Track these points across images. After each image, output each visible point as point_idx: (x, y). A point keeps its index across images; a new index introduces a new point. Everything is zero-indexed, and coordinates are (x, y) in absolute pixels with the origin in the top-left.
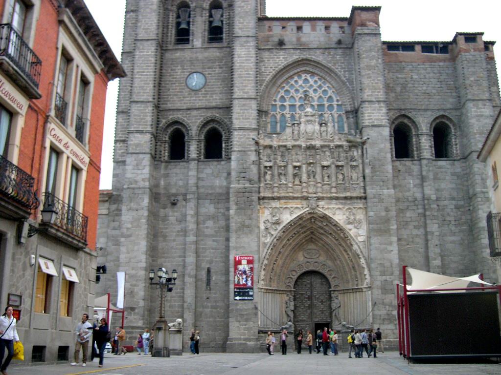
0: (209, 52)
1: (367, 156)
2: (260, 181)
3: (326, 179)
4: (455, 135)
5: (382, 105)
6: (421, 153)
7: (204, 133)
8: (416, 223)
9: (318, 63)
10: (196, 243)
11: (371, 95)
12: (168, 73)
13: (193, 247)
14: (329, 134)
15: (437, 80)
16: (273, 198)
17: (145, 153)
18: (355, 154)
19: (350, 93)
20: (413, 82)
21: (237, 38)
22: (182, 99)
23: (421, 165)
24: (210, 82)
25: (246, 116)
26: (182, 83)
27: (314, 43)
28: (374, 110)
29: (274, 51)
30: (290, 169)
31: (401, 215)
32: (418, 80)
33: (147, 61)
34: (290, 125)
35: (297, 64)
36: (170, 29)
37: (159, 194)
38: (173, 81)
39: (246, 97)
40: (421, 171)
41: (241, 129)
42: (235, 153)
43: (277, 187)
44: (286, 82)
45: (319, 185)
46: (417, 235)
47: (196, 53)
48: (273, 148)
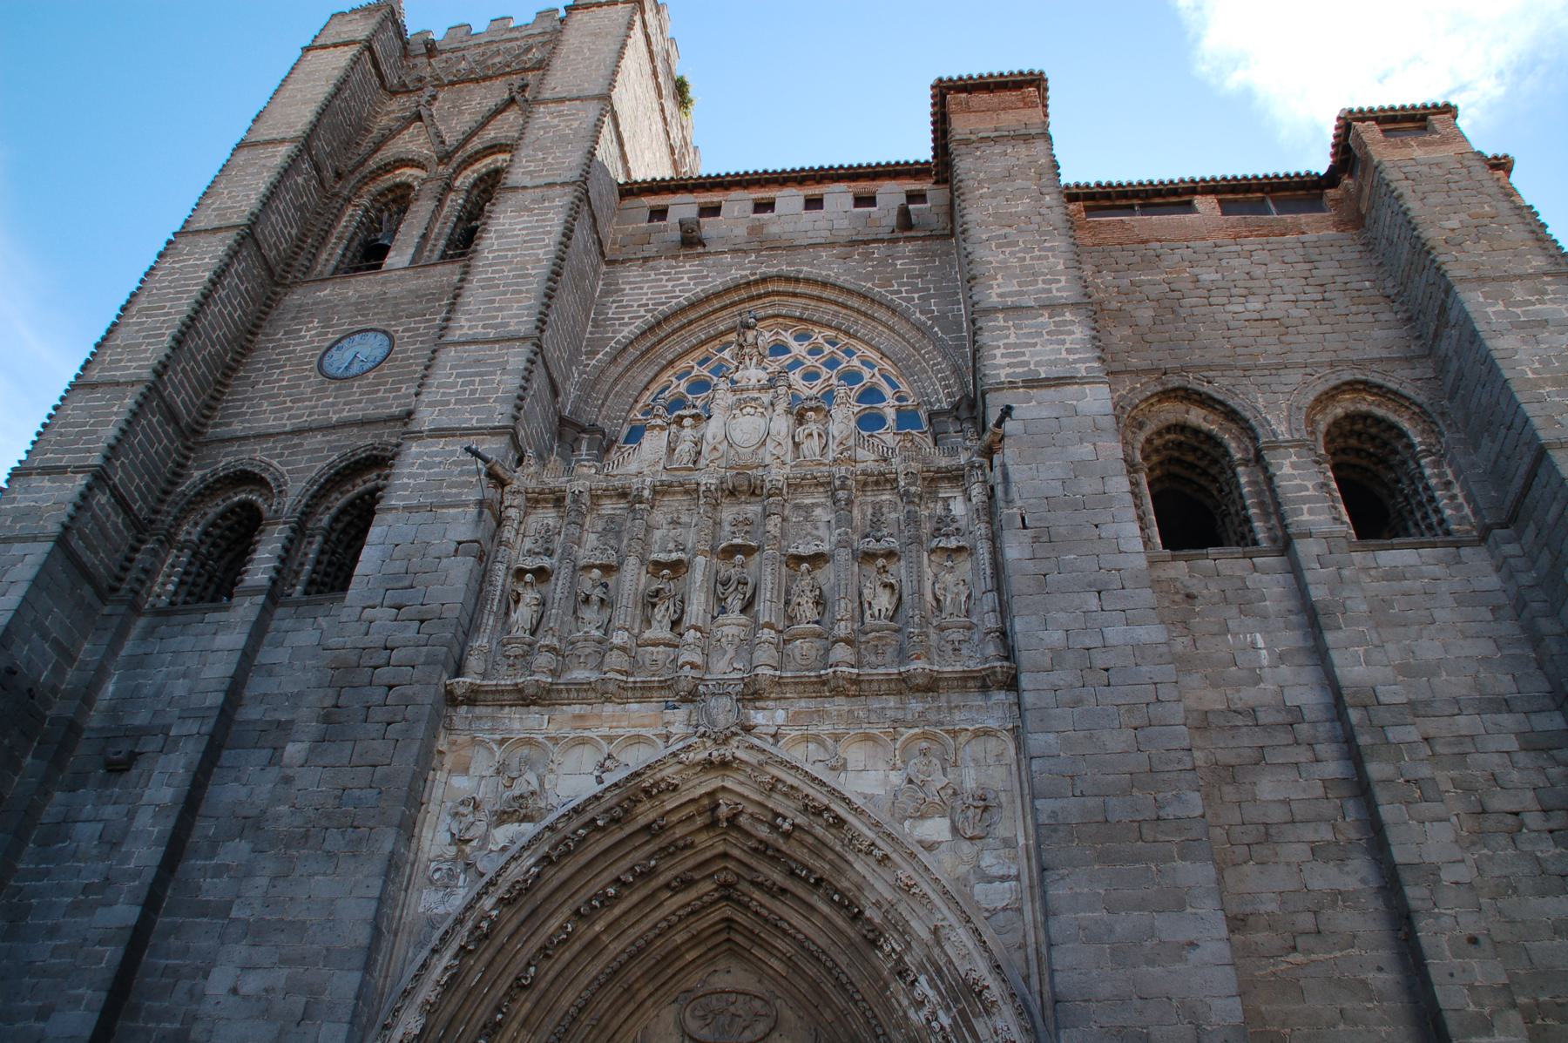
0: (426, 277)
1: (1006, 492)
2: (471, 627)
3: (808, 610)
4: (1429, 453)
5: (1068, 316)
6: (1282, 518)
7: (333, 511)
8: (1326, 833)
9: (824, 284)
10: (139, 939)
11: (1021, 294)
12: (270, 341)
13: (111, 955)
14: (832, 445)
15: (1303, 282)
16: (525, 699)
17: (35, 539)
18: (958, 508)
19: (944, 358)
20: (1205, 293)
21: (509, 195)
22: (289, 404)
23: (1295, 570)
24: (405, 351)
25: (473, 392)
26: (308, 363)
27: (810, 234)
28: (1040, 335)
29: (663, 263)
30: (633, 579)
31: (1229, 792)
32: (1220, 284)
33: (185, 279)
34: (659, 422)
35: (744, 294)
36: (330, 245)
37: (73, 728)
38: (279, 360)
39: (492, 333)
40: (1302, 590)
41: (439, 433)
42: (390, 517)
43: (552, 649)
44: (699, 354)
45: (767, 634)
46: (1336, 895)
47: (384, 284)
48: (568, 501)
